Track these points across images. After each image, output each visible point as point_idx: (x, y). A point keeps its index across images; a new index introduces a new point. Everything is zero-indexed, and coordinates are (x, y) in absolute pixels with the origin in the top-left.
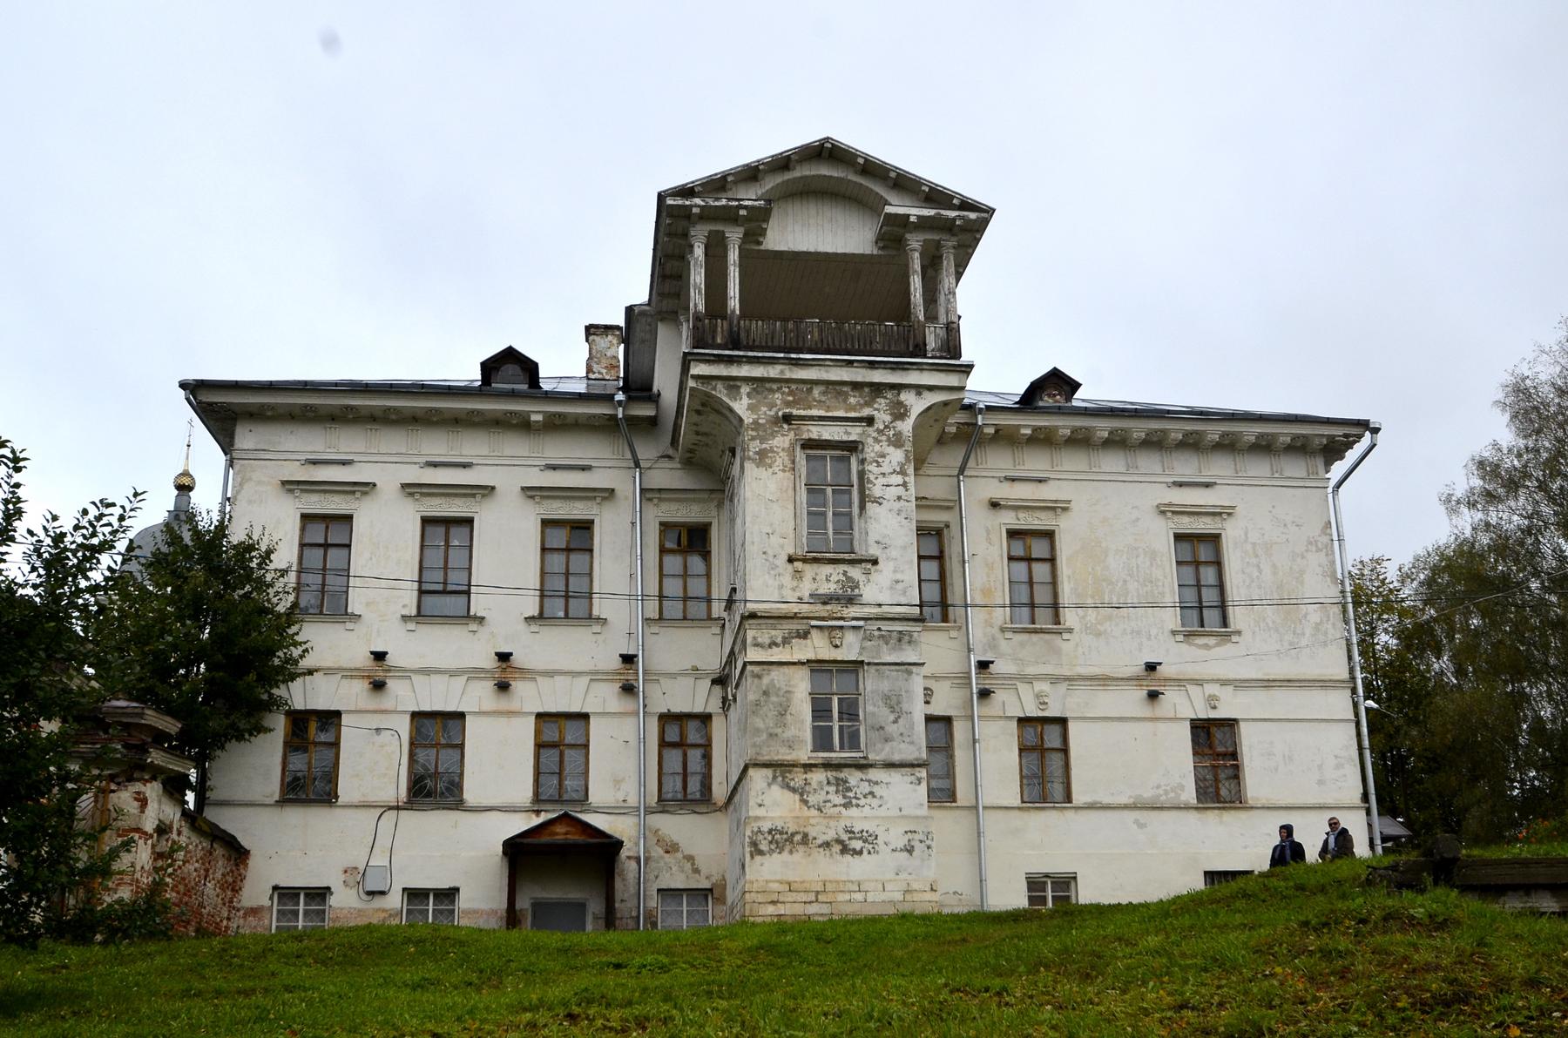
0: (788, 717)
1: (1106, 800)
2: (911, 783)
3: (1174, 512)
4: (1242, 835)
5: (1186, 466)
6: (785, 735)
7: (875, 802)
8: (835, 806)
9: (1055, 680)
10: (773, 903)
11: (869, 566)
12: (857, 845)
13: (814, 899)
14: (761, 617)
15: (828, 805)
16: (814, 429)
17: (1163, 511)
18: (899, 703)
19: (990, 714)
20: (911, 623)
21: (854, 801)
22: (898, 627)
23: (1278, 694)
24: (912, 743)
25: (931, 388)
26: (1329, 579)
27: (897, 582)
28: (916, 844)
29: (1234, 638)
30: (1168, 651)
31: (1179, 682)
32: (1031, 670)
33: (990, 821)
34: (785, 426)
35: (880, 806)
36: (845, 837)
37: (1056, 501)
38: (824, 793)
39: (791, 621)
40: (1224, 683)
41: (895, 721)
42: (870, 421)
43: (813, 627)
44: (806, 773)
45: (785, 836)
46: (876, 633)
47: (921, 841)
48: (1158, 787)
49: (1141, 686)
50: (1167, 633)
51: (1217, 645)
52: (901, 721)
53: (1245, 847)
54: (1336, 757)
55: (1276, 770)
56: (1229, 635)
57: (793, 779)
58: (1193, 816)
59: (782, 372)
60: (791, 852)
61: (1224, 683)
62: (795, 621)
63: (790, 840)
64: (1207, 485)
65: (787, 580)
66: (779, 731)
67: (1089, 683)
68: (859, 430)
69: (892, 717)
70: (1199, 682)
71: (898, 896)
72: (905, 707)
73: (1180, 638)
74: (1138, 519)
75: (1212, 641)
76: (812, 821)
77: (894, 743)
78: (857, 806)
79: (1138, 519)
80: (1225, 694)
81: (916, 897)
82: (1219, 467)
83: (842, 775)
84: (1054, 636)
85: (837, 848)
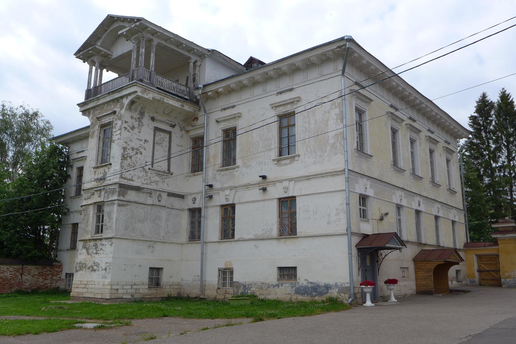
0: (88, 223)
1: (246, 237)
2: (110, 245)
3: (276, 107)
5: (284, 83)
6: (87, 230)
8: (94, 254)
9: (231, 188)
10: (77, 288)
11: (109, 166)
12: (95, 267)
13: (84, 287)
14: (85, 190)
15: (93, 253)
16: (103, 120)
17: (275, 106)
18: (111, 215)
19: (213, 205)
20: (115, 185)
22: (113, 187)
23: (313, 182)
25: (130, 94)
26: (339, 121)
28: (107, 267)
29: (296, 158)
31: (274, 182)
32: (225, 186)
33: (210, 248)
34: (98, 121)
35: (103, 253)
37: (234, 115)
42: (115, 112)
43: (95, 191)
46: (109, 190)
47: (109, 266)
48: (264, 230)
49: (260, 186)
50: (271, 161)
51: (290, 163)
52: (110, 221)
53: (294, 256)
54: (337, 209)
56: (294, 157)
58: (275, 242)
59: (96, 103)
61: (290, 180)
62: (92, 189)
63: (82, 266)
64: (291, 90)
65: (93, 176)
66: (86, 228)
67: (242, 188)
68: (112, 117)
69: (109, 221)
70: (281, 181)
71: (101, 286)
73: (276, 162)
75: (288, 161)
76: (88, 259)
77: (108, 230)
78: (99, 254)
82: (298, 78)
83: (97, 242)
84: (233, 170)
85: (91, 269)
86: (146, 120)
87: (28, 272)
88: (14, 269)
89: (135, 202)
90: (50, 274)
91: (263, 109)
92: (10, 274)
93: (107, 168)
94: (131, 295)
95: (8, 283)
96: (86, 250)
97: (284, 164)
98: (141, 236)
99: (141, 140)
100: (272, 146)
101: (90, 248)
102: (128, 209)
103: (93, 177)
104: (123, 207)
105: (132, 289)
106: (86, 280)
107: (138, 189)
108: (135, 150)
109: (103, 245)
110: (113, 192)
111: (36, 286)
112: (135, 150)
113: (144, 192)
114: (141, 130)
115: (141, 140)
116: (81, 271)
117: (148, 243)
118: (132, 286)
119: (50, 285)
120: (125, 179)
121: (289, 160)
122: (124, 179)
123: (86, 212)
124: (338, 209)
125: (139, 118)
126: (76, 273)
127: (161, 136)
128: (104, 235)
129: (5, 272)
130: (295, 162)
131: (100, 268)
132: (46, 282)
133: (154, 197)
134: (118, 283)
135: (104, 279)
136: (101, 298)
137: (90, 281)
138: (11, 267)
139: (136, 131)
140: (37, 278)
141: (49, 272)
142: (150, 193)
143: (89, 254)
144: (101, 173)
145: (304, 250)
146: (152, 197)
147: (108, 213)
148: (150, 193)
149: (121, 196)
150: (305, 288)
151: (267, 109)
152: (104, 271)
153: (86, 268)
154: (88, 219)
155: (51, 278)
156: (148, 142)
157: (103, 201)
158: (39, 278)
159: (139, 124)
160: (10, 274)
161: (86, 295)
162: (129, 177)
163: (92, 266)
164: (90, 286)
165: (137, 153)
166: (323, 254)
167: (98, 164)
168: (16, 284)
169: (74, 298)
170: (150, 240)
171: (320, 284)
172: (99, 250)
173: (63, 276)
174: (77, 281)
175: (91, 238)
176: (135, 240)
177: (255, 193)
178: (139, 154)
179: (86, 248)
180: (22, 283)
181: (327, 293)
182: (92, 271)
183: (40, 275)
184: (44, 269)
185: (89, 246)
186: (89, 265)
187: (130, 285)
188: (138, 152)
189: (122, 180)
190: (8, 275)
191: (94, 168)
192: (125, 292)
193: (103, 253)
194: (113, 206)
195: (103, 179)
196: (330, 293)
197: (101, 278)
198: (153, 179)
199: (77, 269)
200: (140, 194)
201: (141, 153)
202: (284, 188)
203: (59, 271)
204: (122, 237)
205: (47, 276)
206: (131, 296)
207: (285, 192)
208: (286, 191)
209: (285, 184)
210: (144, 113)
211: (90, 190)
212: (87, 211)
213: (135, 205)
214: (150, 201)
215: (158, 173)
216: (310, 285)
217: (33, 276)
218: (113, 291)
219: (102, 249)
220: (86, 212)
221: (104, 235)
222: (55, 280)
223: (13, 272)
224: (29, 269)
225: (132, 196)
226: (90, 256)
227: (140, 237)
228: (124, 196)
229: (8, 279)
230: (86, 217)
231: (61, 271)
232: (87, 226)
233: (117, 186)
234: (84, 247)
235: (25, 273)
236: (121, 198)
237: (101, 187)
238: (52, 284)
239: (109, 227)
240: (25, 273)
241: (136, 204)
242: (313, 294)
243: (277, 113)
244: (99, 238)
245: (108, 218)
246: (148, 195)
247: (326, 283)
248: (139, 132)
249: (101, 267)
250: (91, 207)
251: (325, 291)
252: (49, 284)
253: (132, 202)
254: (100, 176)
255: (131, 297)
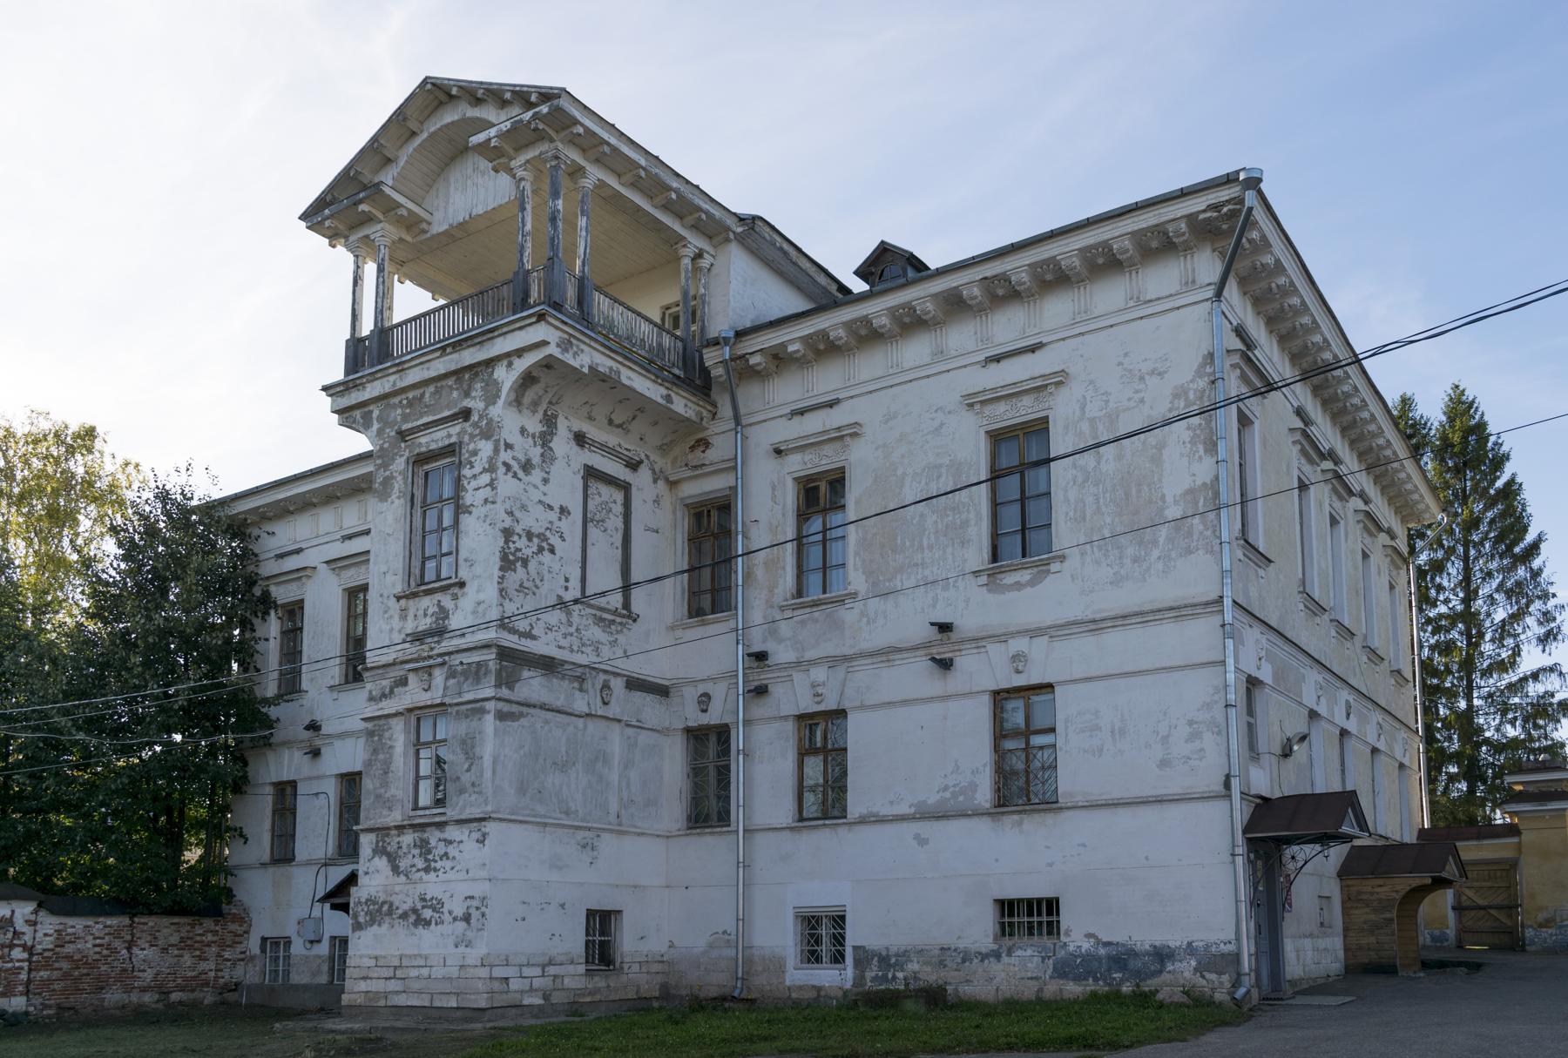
0: (390, 775)
2: (477, 841)
4: (1047, 847)
6: (387, 795)
7: (448, 864)
8: (418, 870)
10: (365, 978)
12: (427, 913)
13: (392, 974)
15: (414, 869)
17: (976, 402)
18: (473, 747)
21: (433, 864)
22: (475, 657)
24: (480, 793)
27: (479, 604)
28: (472, 911)
29: (1054, 567)
30: (967, 601)
35: (453, 868)
36: (419, 906)
38: (410, 856)
39: (393, 668)
40: (1034, 633)
41: (468, 770)
44: (399, 836)
45: (376, 907)
46: (459, 668)
47: (477, 908)
51: (1032, 583)
52: (474, 767)
55: (1101, 750)
57: (389, 843)
60: (380, 925)
61: (1034, 633)
62: (397, 667)
63: (379, 911)
65: (396, 623)
66: (382, 791)
69: (466, 766)
70: (1002, 638)
71: (454, 972)
72: (477, 750)
73: (984, 579)
74: (942, 424)
75: (1024, 576)
76: (397, 889)
77: (467, 795)
78: (435, 870)
79: (942, 424)
80: (1037, 648)
81: (471, 972)
83: (426, 835)
85: (412, 918)
86: (562, 444)
87: (149, 938)
88: (107, 930)
89: (543, 707)
90: (214, 942)
91: (936, 411)
92: (95, 946)
93: (449, 597)
94: (544, 994)
95: (89, 975)
96: (389, 861)
97: (1011, 585)
98: (561, 813)
99: (551, 508)
100: (970, 529)
101: (400, 853)
102: (523, 727)
103: (397, 628)
104: (509, 723)
105: (543, 976)
106: (398, 953)
107: (548, 665)
108: (536, 540)
109: (451, 842)
110: (476, 673)
111: (174, 981)
112: (536, 540)
113: (563, 678)
114: (548, 473)
115: (551, 508)
116: (375, 927)
117: (581, 834)
118: (543, 967)
119: (216, 977)
120: (513, 631)
121: (1029, 571)
122: (510, 632)
123: (380, 740)
124: (1196, 723)
125: (543, 435)
126: (358, 934)
127: (606, 494)
128: (451, 812)
129: (79, 938)
130: (1050, 578)
131: (447, 914)
132: (203, 966)
133: (591, 691)
134: (507, 960)
135: (462, 949)
136: (458, 1008)
137: (410, 956)
138: (97, 923)
139: (536, 476)
140: (176, 956)
141: (210, 937)
142: (581, 677)
143: (398, 874)
144: (425, 615)
145: (1084, 845)
146: (586, 691)
147: (464, 742)
148: (581, 680)
149: (504, 688)
150: (1088, 958)
151: (949, 412)
152: (463, 925)
153: (394, 916)
154: (387, 764)
155: (219, 955)
156: (569, 513)
157: (443, 704)
158: (182, 956)
159: (542, 455)
160: (95, 946)
161: (402, 1000)
162: (522, 625)
163: (415, 911)
164: (414, 973)
165: (541, 550)
166: (1147, 858)
167: (413, 583)
168: (113, 975)
169: (356, 1011)
170: (585, 825)
171: (1138, 948)
172: (437, 858)
173: (254, 945)
174: (361, 957)
175: (405, 823)
176: (545, 825)
177: (915, 676)
178: (546, 553)
179: (389, 855)
180: (133, 971)
181: (1161, 972)
182: (416, 924)
183: (185, 944)
184: (197, 927)
185: (400, 848)
186: (406, 907)
187: (539, 965)
188: (544, 544)
189: (505, 635)
190: (87, 946)
191: (399, 598)
192: (528, 988)
193: (453, 868)
194: (480, 719)
195: (439, 632)
196: (1169, 972)
197: (453, 946)
198: (587, 634)
199: (361, 919)
200: (555, 680)
201: (552, 551)
202: (1016, 657)
203: (239, 932)
204: (513, 817)
205: (207, 949)
206: (544, 999)
207: (1018, 672)
208: (1020, 668)
209: (1018, 645)
210: (556, 417)
211: (389, 669)
212: (381, 736)
213: (543, 714)
214: (580, 705)
215: (598, 613)
216: (1102, 951)
217: (165, 950)
218: (496, 986)
219: (446, 854)
220: (380, 740)
221: (451, 812)
222: (230, 960)
223: (103, 938)
224: (152, 927)
225: (533, 686)
226: (403, 878)
227: (559, 815)
228: (511, 688)
229: (90, 961)
230: (381, 756)
231: (247, 932)
232: (385, 784)
233: (490, 656)
234: (380, 851)
235: (139, 942)
236: (505, 692)
237: (430, 657)
238: (220, 974)
239: (468, 785)
240: (139, 942)
241: (544, 712)
242: (1115, 975)
243: (985, 423)
244: (437, 819)
245: (462, 757)
246: (576, 685)
247: (1157, 944)
248: (546, 481)
249: (450, 913)
250: (398, 726)
251: (1153, 968)
252: (212, 974)
253: (535, 706)
254: (425, 624)
255: (542, 1002)
